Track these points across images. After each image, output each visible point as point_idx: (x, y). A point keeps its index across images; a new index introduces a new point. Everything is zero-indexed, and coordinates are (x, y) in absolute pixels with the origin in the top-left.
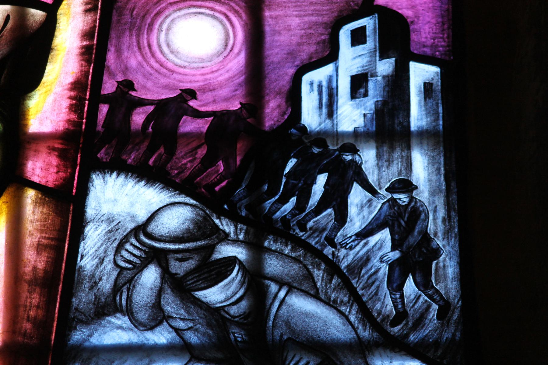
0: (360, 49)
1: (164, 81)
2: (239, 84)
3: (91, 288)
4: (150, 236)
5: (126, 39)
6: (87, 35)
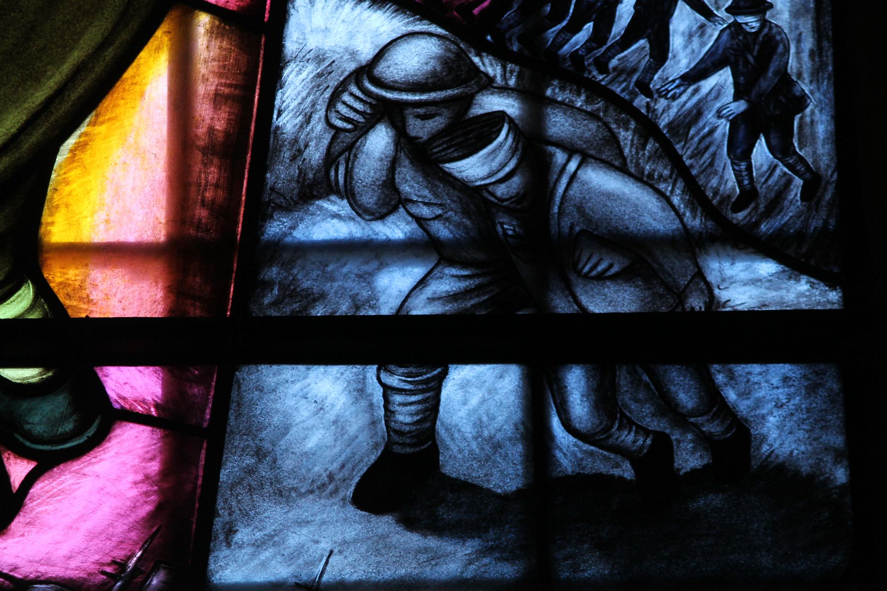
3: (293, 158)
4: (378, 82)
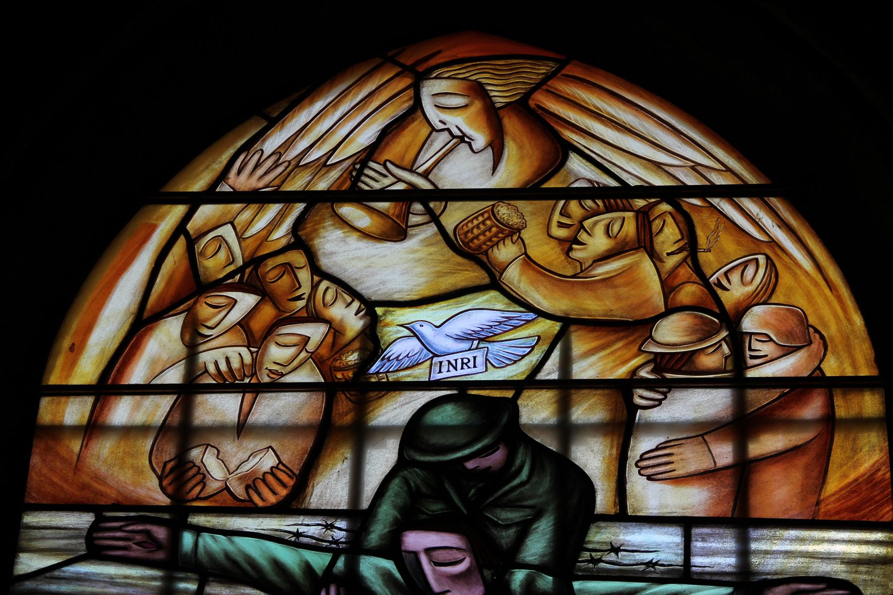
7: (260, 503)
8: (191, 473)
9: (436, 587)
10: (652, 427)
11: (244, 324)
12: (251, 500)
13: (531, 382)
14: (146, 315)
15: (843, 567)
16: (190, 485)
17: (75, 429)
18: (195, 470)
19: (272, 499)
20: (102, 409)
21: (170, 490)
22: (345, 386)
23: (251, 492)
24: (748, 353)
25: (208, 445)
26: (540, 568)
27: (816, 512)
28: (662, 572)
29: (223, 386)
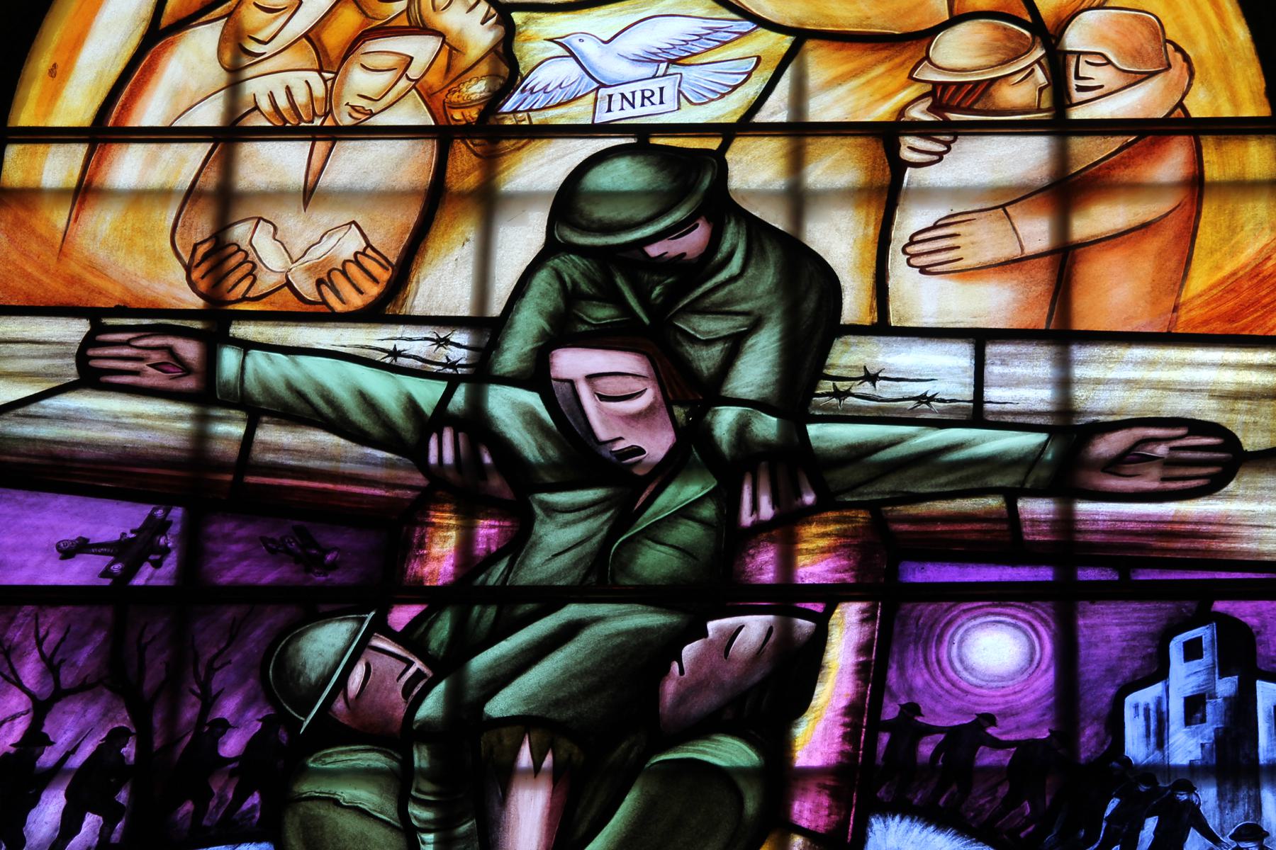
0: (1195, 665)
1: (956, 704)
2: (1048, 707)
5: (910, 654)
6: (863, 649)
7: (339, 307)
8: (234, 261)
9: (602, 433)
10: (927, 194)
11: (312, 37)
12: (325, 302)
13: (746, 126)
14: (165, 22)
15: (1213, 404)
16: (233, 279)
17: (59, 193)
18: (239, 257)
19: (357, 302)
20: (99, 164)
21: (203, 286)
22: (466, 131)
23: (325, 289)
24: (1074, 83)
25: (260, 219)
26: (760, 405)
27: (1173, 322)
28: (941, 412)
29: (281, 132)
